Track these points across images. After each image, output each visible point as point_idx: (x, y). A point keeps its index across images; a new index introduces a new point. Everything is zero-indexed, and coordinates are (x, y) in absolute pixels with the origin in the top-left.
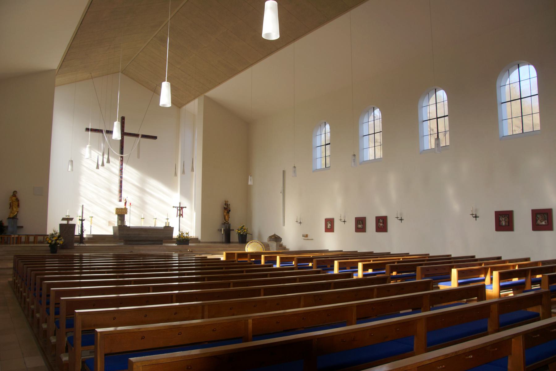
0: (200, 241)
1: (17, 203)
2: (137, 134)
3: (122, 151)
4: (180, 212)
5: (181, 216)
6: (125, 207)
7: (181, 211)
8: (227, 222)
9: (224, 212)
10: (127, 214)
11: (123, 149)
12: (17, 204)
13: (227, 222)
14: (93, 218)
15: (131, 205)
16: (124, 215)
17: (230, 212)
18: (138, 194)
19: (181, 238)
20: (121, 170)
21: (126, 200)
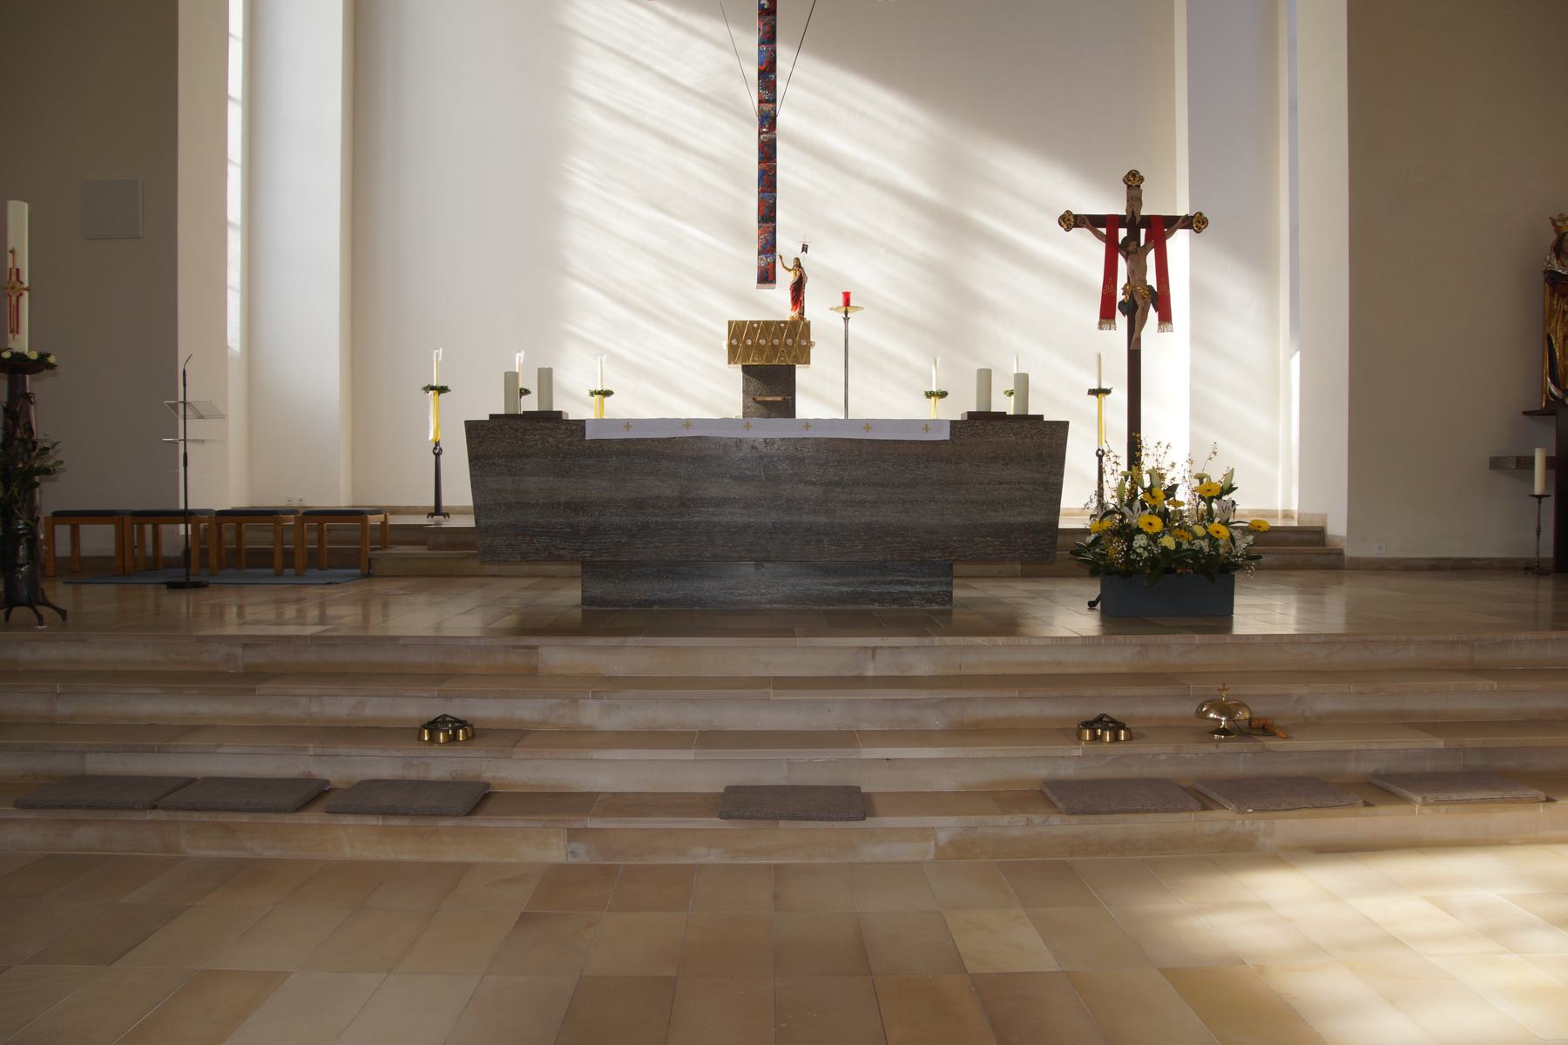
0: (1340, 553)
4: (1137, 272)
5: (1153, 315)
6: (795, 314)
7: (1151, 258)
10: (807, 362)
14: (607, 400)
15: (852, 303)
16: (795, 366)
18: (917, 244)
19: (1140, 541)
20: (767, 72)
21: (798, 265)
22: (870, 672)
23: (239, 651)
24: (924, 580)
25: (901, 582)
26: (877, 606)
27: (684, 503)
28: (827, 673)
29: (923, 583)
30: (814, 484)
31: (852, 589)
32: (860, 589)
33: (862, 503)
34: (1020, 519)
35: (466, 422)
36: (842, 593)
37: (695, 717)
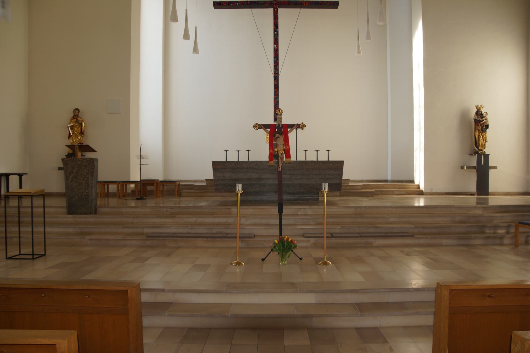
0: (422, 191)
1: (79, 128)
2: (301, 1)
3: (276, 33)
8: (481, 150)
9: (475, 129)
11: (278, 29)
12: (80, 131)
13: (481, 150)
17: (487, 130)
22: (299, 213)
23: (169, 210)
24: (312, 196)
25: (307, 196)
26: (302, 202)
27: (260, 179)
28: (290, 214)
29: (312, 197)
30: (288, 175)
31: (296, 198)
32: (298, 198)
33: (298, 179)
34: (333, 182)
35: (212, 162)
36: (294, 199)
37: (264, 221)
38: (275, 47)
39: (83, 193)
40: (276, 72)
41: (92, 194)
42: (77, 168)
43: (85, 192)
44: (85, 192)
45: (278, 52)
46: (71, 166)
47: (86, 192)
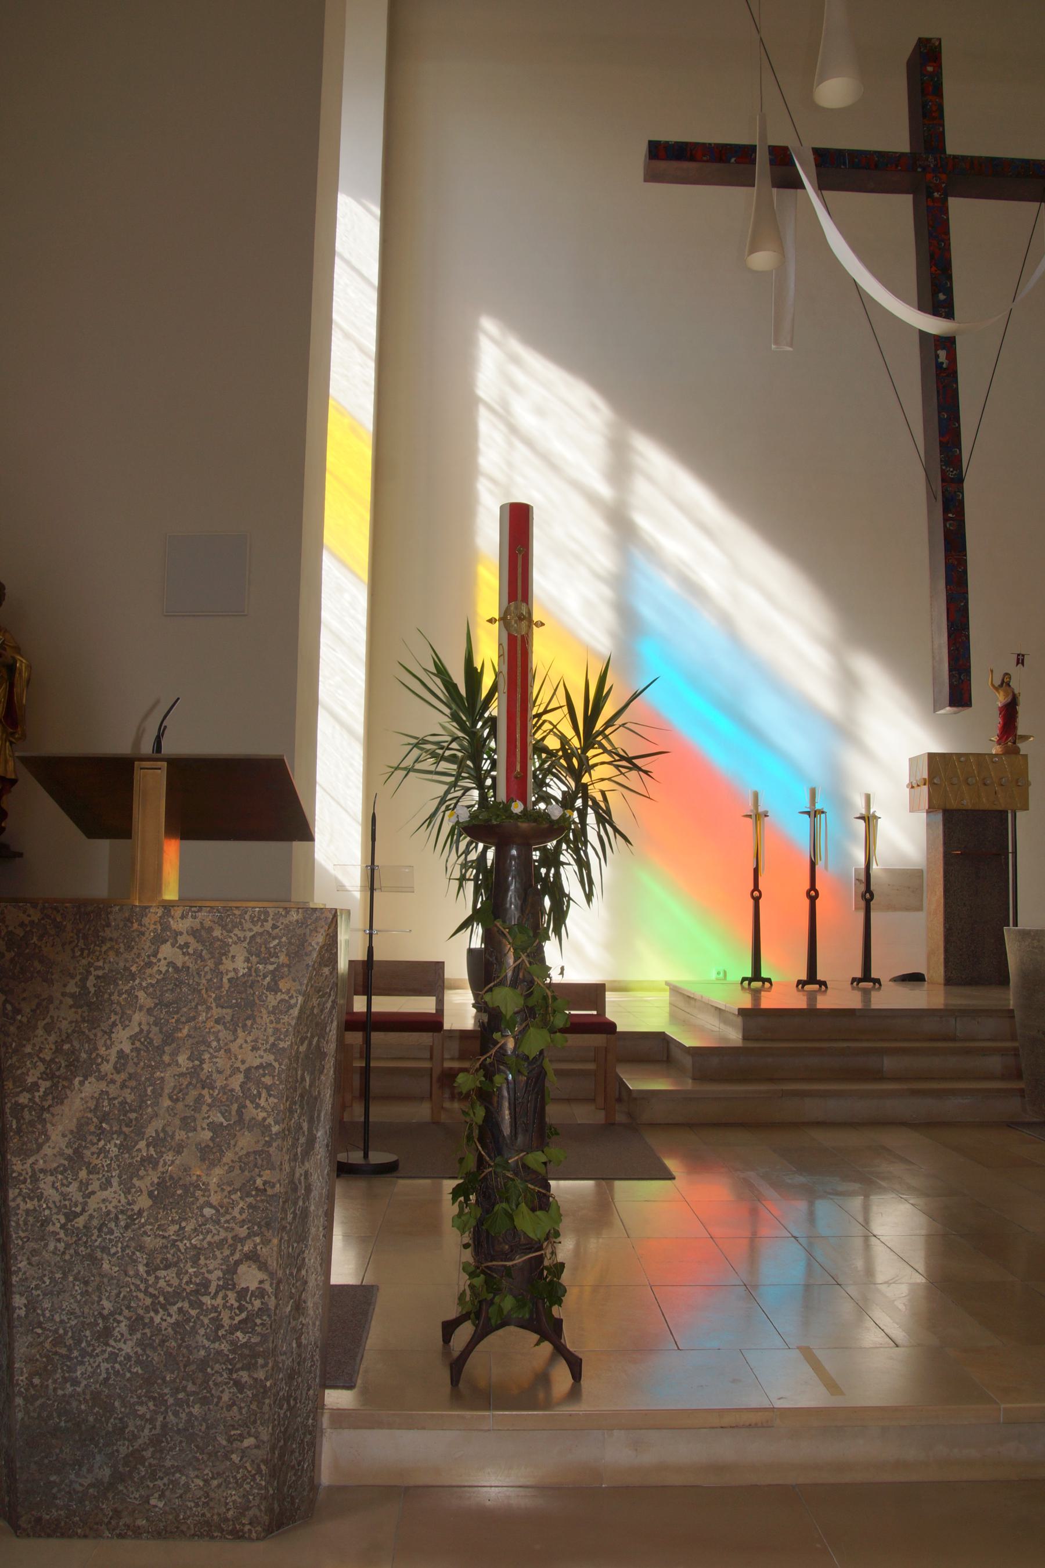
3: (942, 297)
21: (1005, 683)
38: (940, 360)
39: (206, 1300)
40: (952, 474)
41: (299, 1308)
42: (137, 1017)
43: (228, 1282)
44: (228, 1282)
45: (957, 383)
46: (72, 988)
47: (242, 1294)
